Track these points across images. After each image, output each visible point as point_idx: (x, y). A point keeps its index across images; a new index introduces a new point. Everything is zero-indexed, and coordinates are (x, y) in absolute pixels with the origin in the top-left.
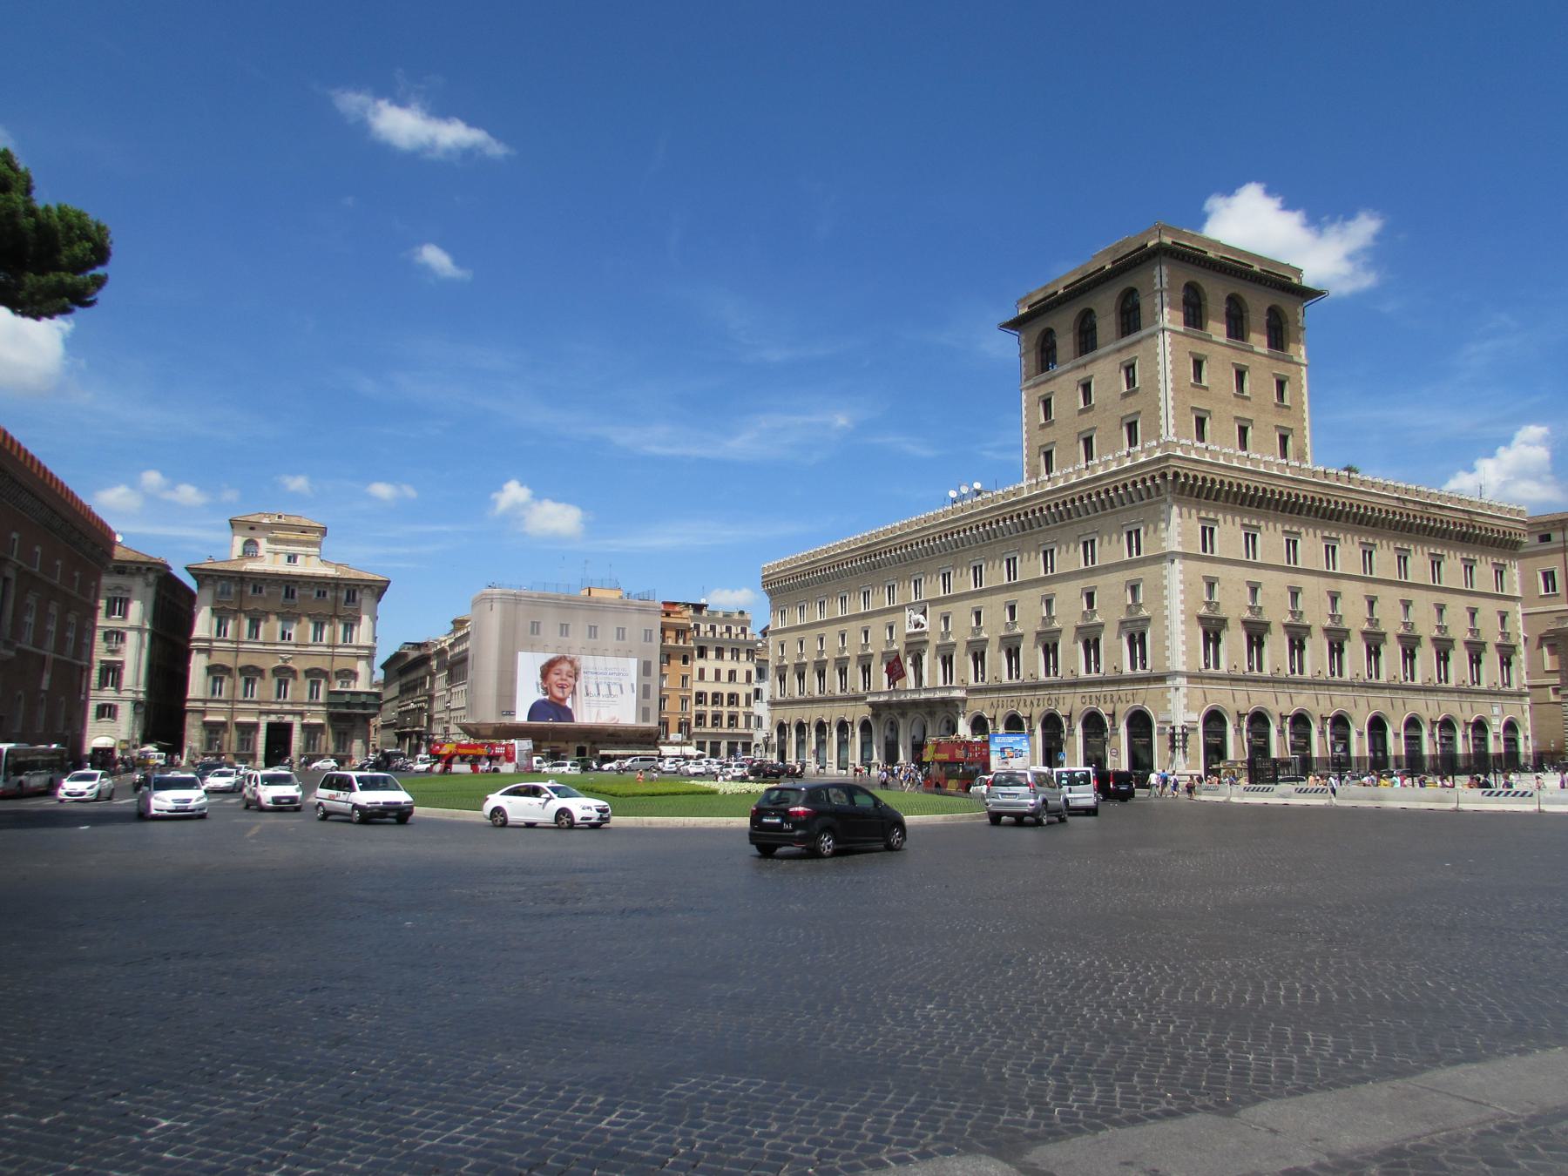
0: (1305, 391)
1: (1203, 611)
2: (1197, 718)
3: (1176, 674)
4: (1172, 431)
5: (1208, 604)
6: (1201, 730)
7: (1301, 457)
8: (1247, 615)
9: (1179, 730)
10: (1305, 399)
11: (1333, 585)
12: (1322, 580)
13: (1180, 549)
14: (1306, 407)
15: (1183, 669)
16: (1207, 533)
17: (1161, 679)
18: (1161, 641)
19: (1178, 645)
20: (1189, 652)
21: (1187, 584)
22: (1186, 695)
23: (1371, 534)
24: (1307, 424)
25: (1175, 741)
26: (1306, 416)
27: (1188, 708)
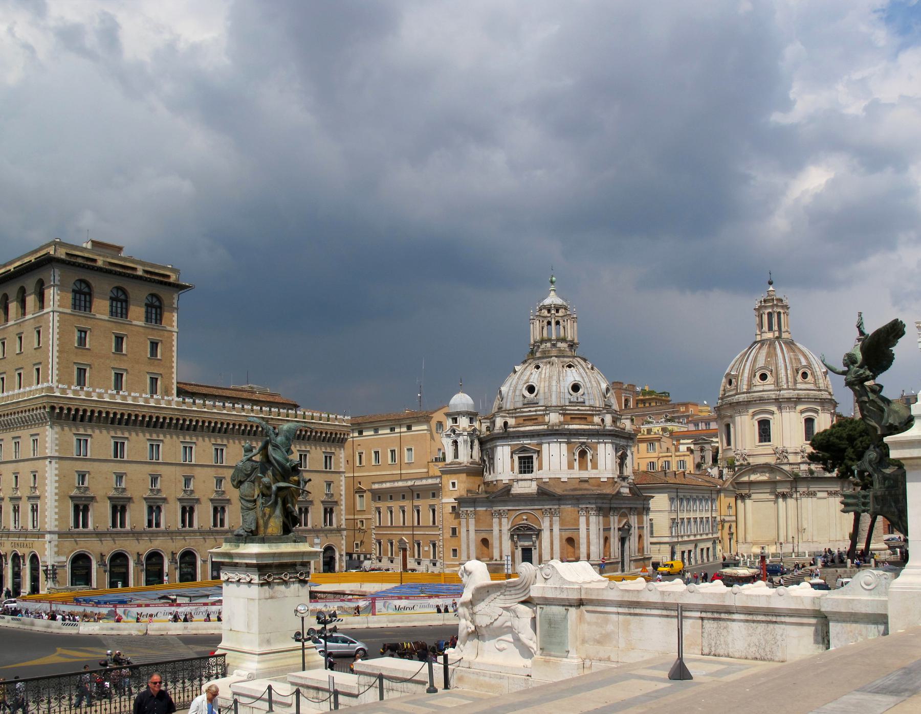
0: (175, 349)
1: (75, 492)
2: (66, 560)
3: (50, 533)
4: (54, 381)
5: (79, 488)
6: (68, 568)
7: (167, 392)
8: (112, 493)
9: (50, 568)
10: (175, 354)
11: (188, 471)
12: (178, 468)
13: (57, 454)
14: (175, 359)
15: (56, 529)
16: (82, 442)
17: (43, 536)
18: (44, 511)
19: (52, 513)
20: (61, 518)
21: (62, 477)
22: (57, 546)
23: (222, 439)
24: (174, 370)
25: (52, 574)
26: (175, 365)
27: (58, 553)
